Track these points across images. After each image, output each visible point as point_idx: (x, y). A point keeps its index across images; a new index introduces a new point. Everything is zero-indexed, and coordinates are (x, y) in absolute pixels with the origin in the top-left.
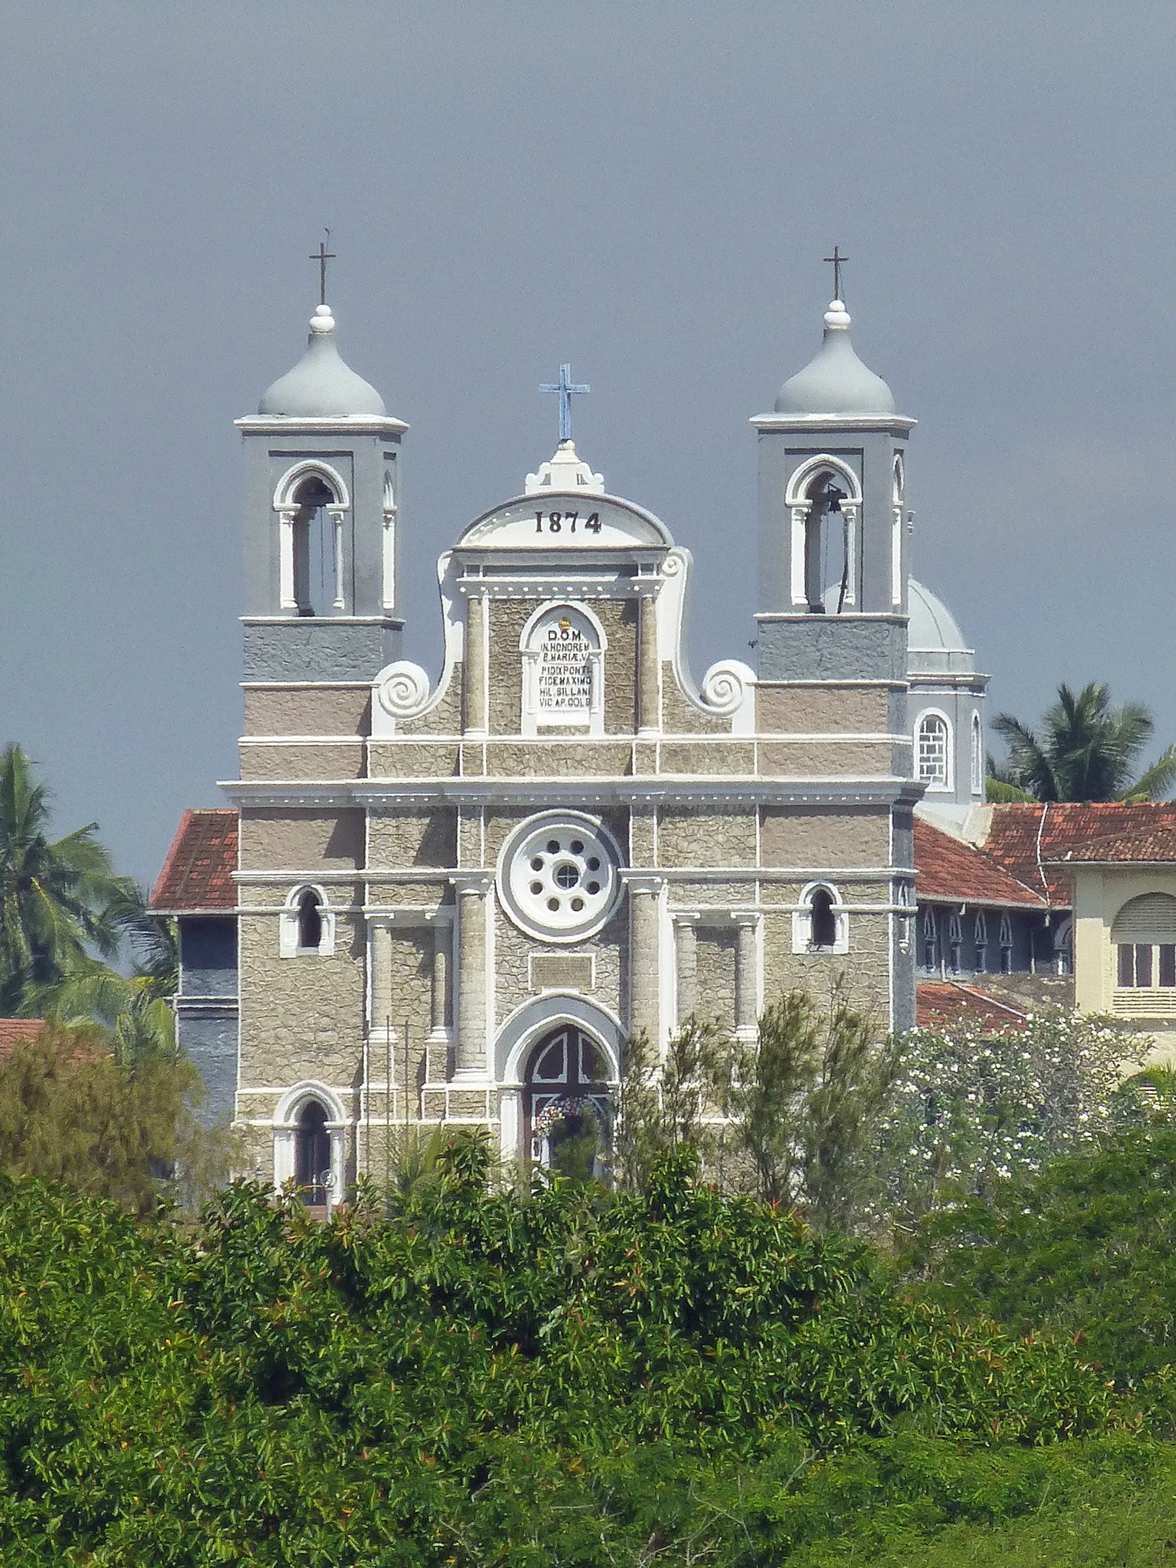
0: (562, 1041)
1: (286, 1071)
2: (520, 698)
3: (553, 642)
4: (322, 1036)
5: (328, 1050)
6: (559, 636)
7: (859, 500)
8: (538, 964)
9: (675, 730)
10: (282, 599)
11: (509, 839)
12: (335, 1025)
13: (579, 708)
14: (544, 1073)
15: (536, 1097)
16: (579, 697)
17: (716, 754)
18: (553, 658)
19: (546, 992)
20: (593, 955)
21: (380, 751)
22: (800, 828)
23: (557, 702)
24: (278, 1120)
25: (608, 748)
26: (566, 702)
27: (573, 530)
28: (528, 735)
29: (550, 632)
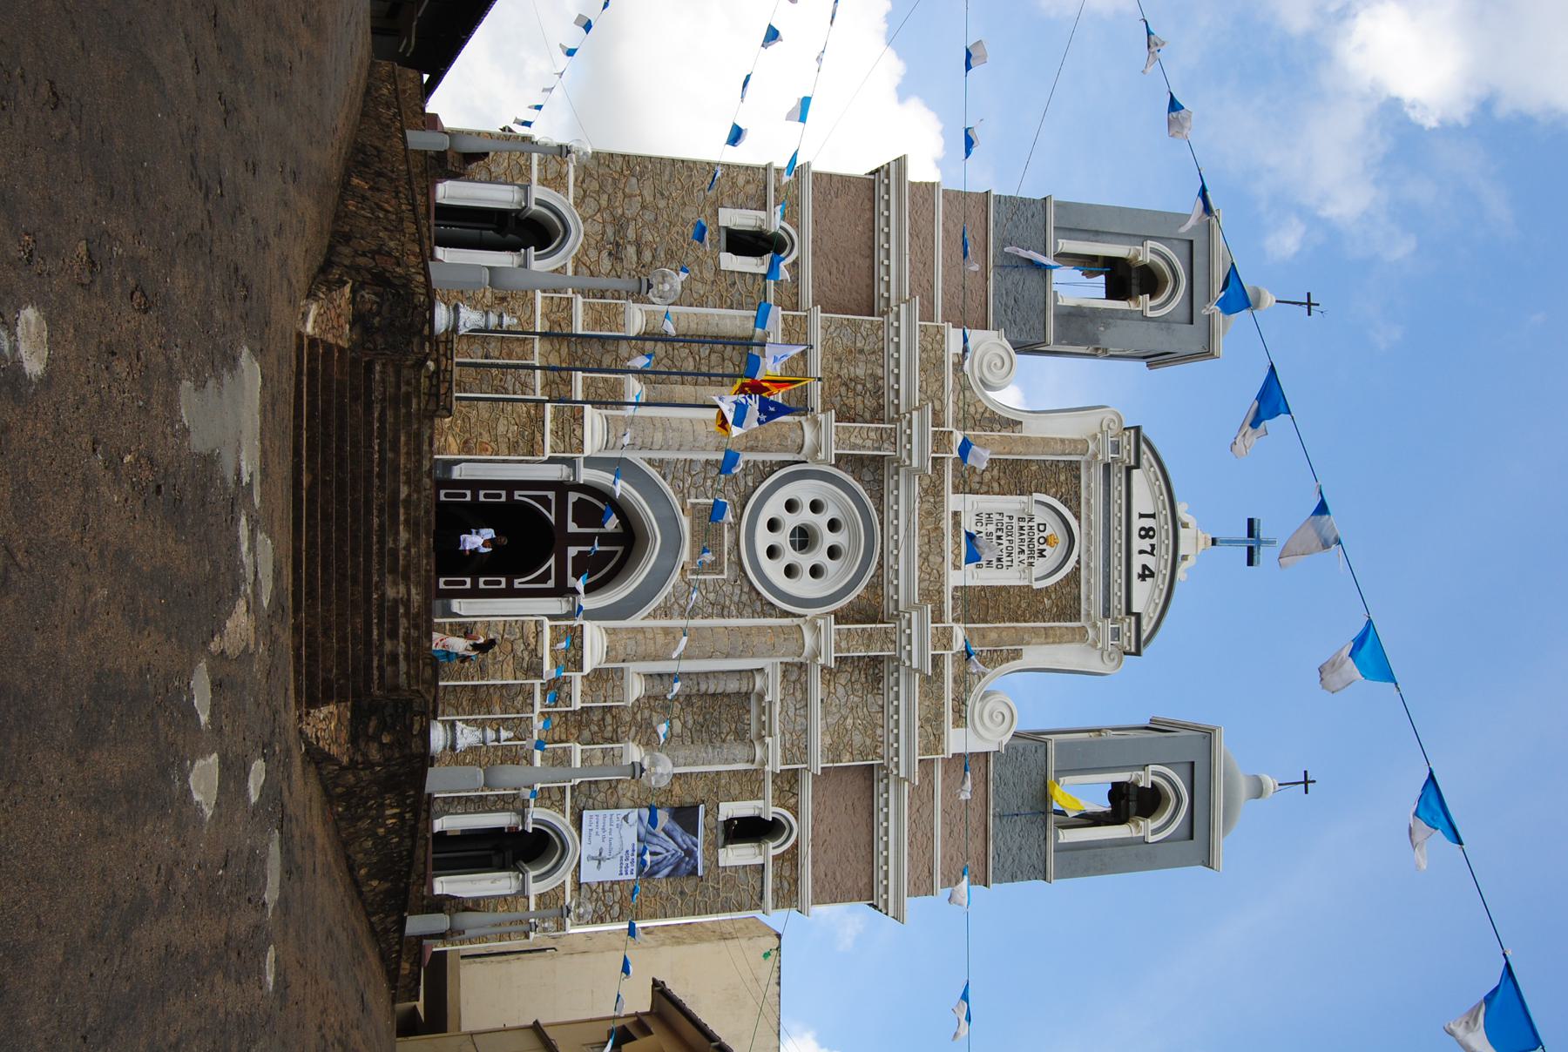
1: (593, 204)
2: (987, 493)
3: (1036, 528)
4: (631, 250)
5: (615, 256)
6: (1041, 534)
11: (849, 479)
12: (643, 266)
15: (551, 495)
19: (685, 523)
20: (725, 577)
21: (938, 337)
24: (538, 192)
25: (940, 592)
27: (1141, 552)
28: (953, 501)
29: (1045, 525)
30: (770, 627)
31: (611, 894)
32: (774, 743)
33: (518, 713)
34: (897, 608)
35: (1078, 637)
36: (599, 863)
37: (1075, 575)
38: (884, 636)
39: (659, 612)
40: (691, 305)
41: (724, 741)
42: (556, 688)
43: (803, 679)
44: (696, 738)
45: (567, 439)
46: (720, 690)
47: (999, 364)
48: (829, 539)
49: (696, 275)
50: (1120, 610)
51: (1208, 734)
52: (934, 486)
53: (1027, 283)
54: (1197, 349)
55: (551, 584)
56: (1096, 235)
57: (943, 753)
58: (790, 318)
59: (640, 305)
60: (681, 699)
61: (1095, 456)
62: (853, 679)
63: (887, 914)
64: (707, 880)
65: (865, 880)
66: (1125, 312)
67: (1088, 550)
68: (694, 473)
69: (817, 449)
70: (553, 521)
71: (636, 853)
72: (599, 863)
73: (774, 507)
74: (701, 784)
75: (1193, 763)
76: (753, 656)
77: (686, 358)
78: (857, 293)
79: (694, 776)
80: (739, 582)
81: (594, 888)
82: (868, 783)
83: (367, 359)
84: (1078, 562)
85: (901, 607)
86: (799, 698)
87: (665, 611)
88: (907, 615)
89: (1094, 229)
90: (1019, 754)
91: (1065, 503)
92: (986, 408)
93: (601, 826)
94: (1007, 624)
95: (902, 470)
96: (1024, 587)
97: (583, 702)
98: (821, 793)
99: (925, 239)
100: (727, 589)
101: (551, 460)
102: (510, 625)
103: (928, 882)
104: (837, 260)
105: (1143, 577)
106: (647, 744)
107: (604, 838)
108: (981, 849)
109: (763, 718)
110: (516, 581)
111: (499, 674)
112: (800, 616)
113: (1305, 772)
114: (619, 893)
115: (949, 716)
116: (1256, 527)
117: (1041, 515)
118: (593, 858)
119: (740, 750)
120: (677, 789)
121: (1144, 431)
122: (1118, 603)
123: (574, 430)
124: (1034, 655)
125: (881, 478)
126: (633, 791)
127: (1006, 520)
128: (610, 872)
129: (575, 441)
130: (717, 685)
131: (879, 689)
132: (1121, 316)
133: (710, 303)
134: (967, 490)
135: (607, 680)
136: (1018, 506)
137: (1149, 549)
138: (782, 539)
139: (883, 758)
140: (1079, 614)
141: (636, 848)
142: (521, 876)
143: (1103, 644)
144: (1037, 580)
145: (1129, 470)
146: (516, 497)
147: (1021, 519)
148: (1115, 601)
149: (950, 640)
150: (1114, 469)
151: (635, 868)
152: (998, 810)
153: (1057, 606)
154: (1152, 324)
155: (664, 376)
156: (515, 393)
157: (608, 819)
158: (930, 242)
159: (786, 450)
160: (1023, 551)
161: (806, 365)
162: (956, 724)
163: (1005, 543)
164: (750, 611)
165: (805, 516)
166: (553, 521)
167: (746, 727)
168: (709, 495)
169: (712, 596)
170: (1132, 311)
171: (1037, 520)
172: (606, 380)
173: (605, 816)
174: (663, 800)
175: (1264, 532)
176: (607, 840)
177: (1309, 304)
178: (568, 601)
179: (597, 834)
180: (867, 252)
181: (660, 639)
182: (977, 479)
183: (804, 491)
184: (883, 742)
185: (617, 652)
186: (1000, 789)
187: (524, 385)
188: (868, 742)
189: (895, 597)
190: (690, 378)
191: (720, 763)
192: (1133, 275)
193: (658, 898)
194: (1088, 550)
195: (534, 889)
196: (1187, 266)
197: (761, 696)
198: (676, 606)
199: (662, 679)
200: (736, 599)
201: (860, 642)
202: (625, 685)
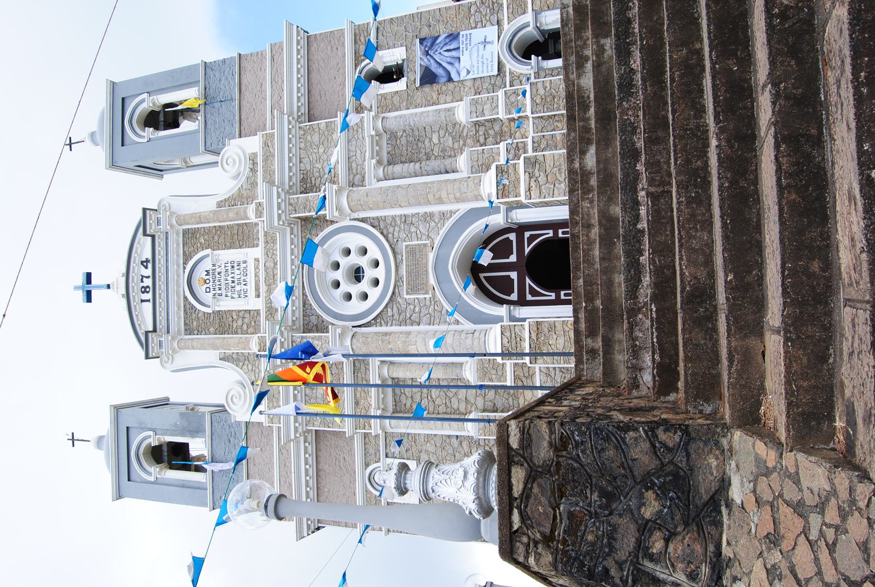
0: (484, 277)
2: (239, 311)
3: (212, 290)
6: (208, 286)
7: (145, 95)
8: (412, 290)
9: (256, 195)
10: (202, 481)
13: (248, 268)
14: (510, 292)
16: (242, 269)
17: (269, 161)
18: (220, 289)
19: (432, 281)
20: (404, 243)
22: (323, 98)
23: (245, 285)
25: (267, 242)
26: (245, 278)
29: (206, 292)
30: (371, 209)
31: (477, 20)
32: (369, 131)
33: (543, 136)
34: (292, 229)
35: (182, 218)
36: (485, 40)
37: (187, 258)
38: (297, 208)
39: (449, 215)
40: (435, 435)
41: (404, 131)
42: (517, 151)
43: (351, 176)
44: (423, 131)
45: (513, 335)
46: (407, 165)
47: (234, 398)
48: (338, 275)
49: (433, 456)
50: (159, 238)
51: (113, 165)
52: (271, 314)
53: (223, 454)
54: (123, 411)
55: (527, 234)
56: (183, 485)
57: (263, 135)
58: (367, 427)
59: (470, 435)
60: (433, 157)
61: (173, 339)
62: (319, 179)
63: (298, 27)
64: (413, 36)
65: (313, 49)
66: (166, 434)
67: (178, 276)
68: (428, 316)
69: (342, 336)
70: (527, 277)
71: (461, 49)
72: (485, 40)
73: (374, 294)
74: (419, 101)
75: (123, 145)
76: (381, 188)
77: (437, 398)
78: (327, 445)
79: (424, 105)
80: (395, 241)
81: (488, 23)
82: (312, 112)
83: (672, 397)
84: (184, 268)
85: (288, 229)
86: (354, 163)
87: (444, 216)
88: (281, 223)
89: (185, 489)
90: (221, 141)
91: (193, 307)
92: (241, 369)
93: (485, 65)
94: (225, 224)
95: (290, 323)
96: (216, 250)
97: (498, 148)
98: (341, 102)
99: (285, 482)
100: (403, 235)
101: (524, 320)
102: (549, 194)
103: (274, 52)
104: (340, 466)
105: (147, 261)
106: (455, 124)
107: (482, 58)
108: (243, 77)
109: (377, 148)
110: (551, 235)
111: (556, 158)
112: (355, 219)
113: (71, 150)
114: (471, 21)
115: (260, 160)
116: (85, 297)
117: (207, 298)
118: (489, 43)
119: (392, 125)
120: (435, 96)
121: (142, 353)
122: (160, 243)
123: (508, 342)
124: (209, 205)
125: (305, 318)
126: (464, 91)
127: (229, 294)
128: (478, 34)
129: (508, 334)
130: (408, 168)
131: (303, 174)
132: (168, 432)
133: (422, 437)
134: (252, 313)
135: (482, 165)
136: (221, 303)
137: (144, 279)
138: (370, 273)
139: (300, 128)
140: (183, 234)
141: (461, 52)
142: (538, 25)
143: (166, 214)
144: (208, 256)
145: (155, 330)
146: (553, 294)
147: (220, 295)
148: (163, 244)
149: (257, 209)
150: (165, 330)
151: (461, 39)
152: (234, 104)
153: (196, 238)
154: (149, 426)
155: (451, 384)
156: (555, 368)
157: (480, 70)
158: (282, 480)
159: (364, 335)
160: (218, 274)
161: (355, 394)
162: (255, 155)
163: (229, 278)
164: (387, 221)
165: (355, 289)
166: (527, 277)
167: (390, 142)
168: (416, 301)
169: (413, 229)
170: (162, 435)
171: (210, 295)
172: (491, 380)
173: (483, 72)
174: (444, 87)
175: (81, 295)
176: (480, 56)
177: (73, 440)
178: (512, 220)
179: (487, 60)
180: (321, 473)
181: (444, 195)
182: (246, 320)
183: (356, 307)
184: (300, 138)
185: (474, 182)
186: (232, 118)
187: (548, 375)
188: (309, 138)
189: (293, 236)
190: (434, 383)
191: (405, 115)
192: (166, 458)
193: (445, 21)
194: (178, 276)
195: (529, 17)
196: (130, 461)
197: (379, 162)
198: (437, 220)
199: (446, 170)
200: (397, 229)
201: (312, 203)
202: (470, 162)
